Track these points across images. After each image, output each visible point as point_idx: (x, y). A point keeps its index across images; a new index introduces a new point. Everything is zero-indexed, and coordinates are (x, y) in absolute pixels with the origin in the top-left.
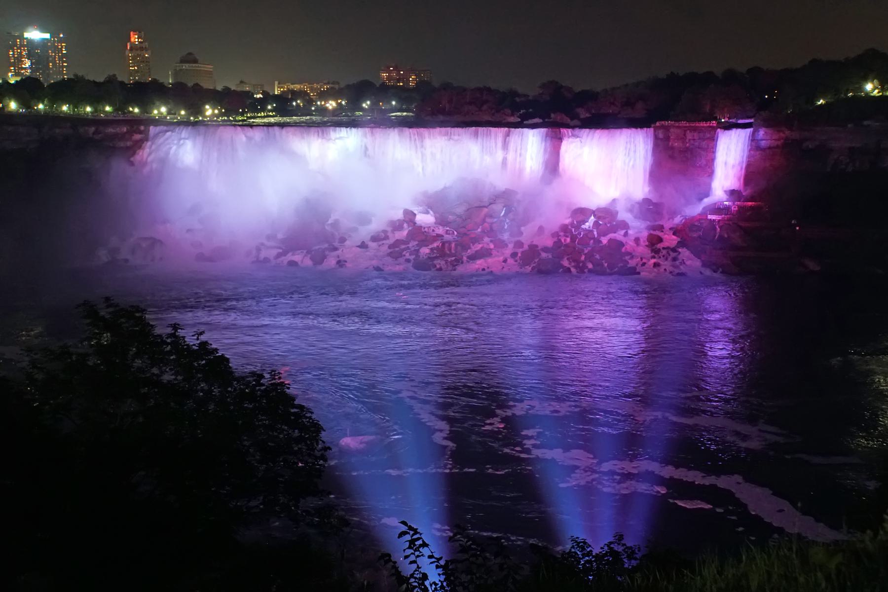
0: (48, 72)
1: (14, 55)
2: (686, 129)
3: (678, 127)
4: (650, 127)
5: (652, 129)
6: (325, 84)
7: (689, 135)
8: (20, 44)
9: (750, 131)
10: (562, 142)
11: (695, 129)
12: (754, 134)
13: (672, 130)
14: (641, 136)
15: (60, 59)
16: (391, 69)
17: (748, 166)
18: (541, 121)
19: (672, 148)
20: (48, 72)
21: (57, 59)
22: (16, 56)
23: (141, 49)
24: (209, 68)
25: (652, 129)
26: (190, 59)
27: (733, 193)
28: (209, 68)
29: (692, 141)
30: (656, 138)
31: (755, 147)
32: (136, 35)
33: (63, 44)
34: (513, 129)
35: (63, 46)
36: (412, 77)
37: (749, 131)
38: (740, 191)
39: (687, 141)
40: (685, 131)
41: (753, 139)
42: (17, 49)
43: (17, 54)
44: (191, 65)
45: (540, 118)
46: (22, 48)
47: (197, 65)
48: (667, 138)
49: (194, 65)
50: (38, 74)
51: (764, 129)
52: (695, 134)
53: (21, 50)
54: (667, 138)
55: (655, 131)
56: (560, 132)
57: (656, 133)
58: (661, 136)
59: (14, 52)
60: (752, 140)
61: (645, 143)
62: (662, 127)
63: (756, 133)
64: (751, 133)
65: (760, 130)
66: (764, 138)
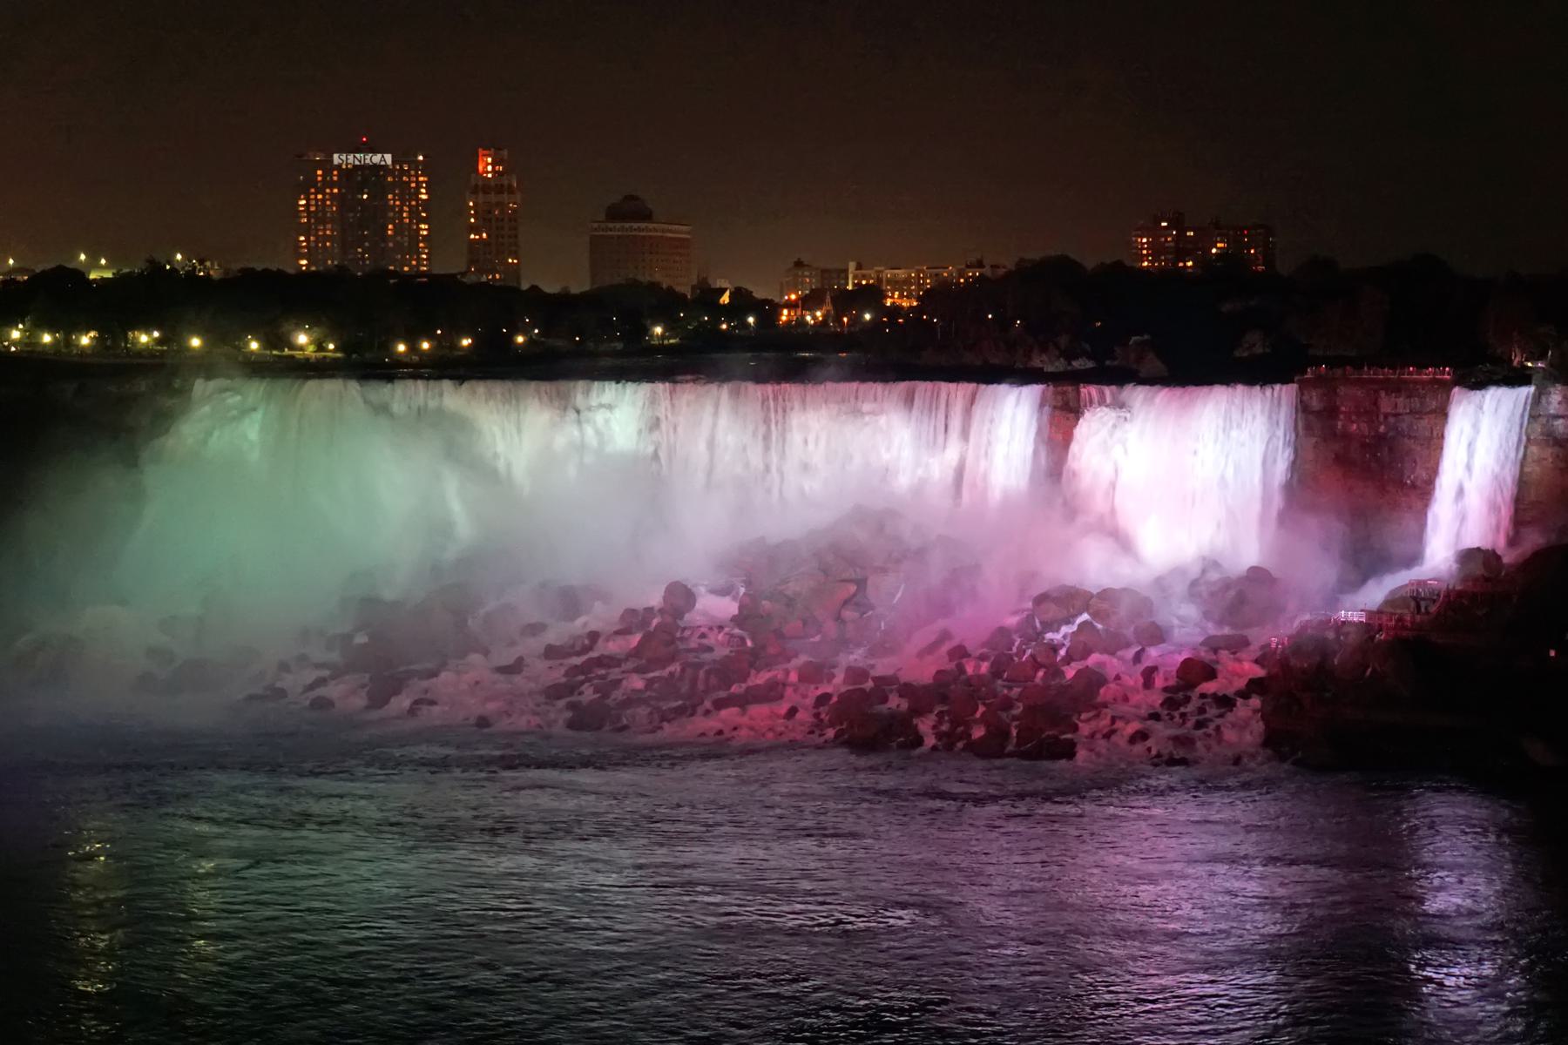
0: (383, 245)
1: (308, 205)
2: (1376, 387)
3: (1360, 382)
4: (1293, 382)
5: (1295, 386)
6: (968, 267)
7: (1386, 404)
8: (324, 180)
9: (1528, 394)
10: (1078, 419)
11: (1397, 388)
12: (1537, 400)
13: (1342, 390)
14: (1258, 407)
15: (414, 213)
16: (1164, 224)
17: (1522, 482)
18: (1090, 364)
19: (1346, 436)
20: (383, 245)
21: (405, 215)
22: (313, 209)
23: (500, 189)
24: (682, 231)
25: (1295, 386)
26: (631, 210)
27: (1468, 556)
28: (682, 231)
29: (1391, 420)
30: (1303, 408)
31: (1542, 434)
32: (490, 156)
33: (421, 179)
34: (983, 387)
35: (423, 182)
36: (1219, 245)
37: (1527, 391)
38: (1494, 552)
39: (1381, 418)
40: (1376, 391)
41: (1535, 410)
42: (316, 194)
43: (316, 205)
44: (627, 225)
45: (1090, 358)
46: (328, 191)
47: (651, 226)
48: (1330, 412)
49: (643, 225)
50: (360, 250)
51: (1559, 387)
52: (1401, 400)
53: (324, 194)
54: (1330, 412)
55: (1301, 389)
56: (1078, 393)
57: (1306, 398)
58: (1316, 404)
59: (308, 200)
60: (1533, 417)
61: (1273, 422)
62: (1319, 381)
63: (1544, 400)
64: (1530, 401)
65: (1552, 390)
66: (1560, 414)
